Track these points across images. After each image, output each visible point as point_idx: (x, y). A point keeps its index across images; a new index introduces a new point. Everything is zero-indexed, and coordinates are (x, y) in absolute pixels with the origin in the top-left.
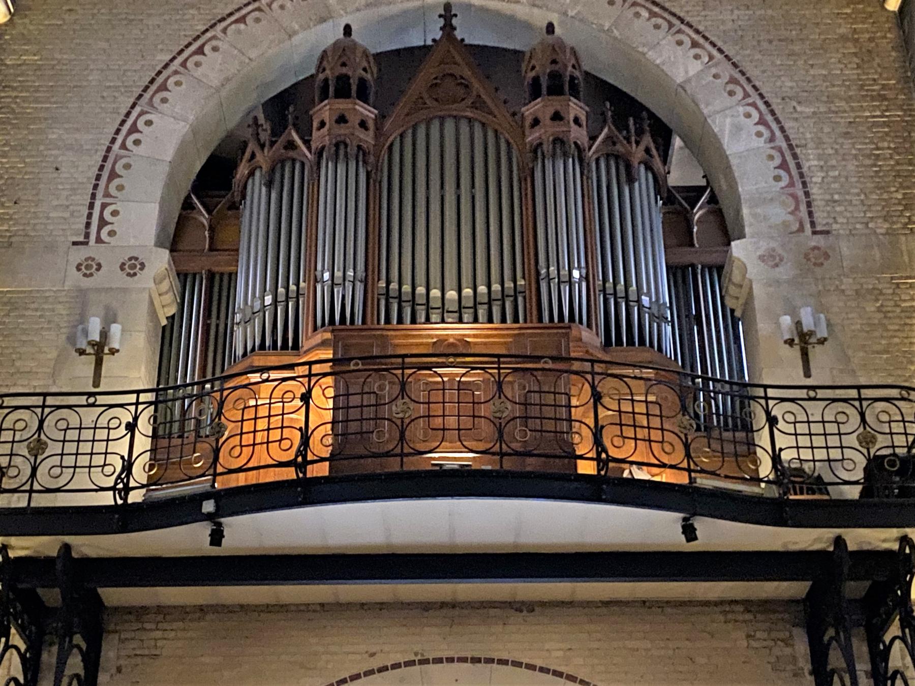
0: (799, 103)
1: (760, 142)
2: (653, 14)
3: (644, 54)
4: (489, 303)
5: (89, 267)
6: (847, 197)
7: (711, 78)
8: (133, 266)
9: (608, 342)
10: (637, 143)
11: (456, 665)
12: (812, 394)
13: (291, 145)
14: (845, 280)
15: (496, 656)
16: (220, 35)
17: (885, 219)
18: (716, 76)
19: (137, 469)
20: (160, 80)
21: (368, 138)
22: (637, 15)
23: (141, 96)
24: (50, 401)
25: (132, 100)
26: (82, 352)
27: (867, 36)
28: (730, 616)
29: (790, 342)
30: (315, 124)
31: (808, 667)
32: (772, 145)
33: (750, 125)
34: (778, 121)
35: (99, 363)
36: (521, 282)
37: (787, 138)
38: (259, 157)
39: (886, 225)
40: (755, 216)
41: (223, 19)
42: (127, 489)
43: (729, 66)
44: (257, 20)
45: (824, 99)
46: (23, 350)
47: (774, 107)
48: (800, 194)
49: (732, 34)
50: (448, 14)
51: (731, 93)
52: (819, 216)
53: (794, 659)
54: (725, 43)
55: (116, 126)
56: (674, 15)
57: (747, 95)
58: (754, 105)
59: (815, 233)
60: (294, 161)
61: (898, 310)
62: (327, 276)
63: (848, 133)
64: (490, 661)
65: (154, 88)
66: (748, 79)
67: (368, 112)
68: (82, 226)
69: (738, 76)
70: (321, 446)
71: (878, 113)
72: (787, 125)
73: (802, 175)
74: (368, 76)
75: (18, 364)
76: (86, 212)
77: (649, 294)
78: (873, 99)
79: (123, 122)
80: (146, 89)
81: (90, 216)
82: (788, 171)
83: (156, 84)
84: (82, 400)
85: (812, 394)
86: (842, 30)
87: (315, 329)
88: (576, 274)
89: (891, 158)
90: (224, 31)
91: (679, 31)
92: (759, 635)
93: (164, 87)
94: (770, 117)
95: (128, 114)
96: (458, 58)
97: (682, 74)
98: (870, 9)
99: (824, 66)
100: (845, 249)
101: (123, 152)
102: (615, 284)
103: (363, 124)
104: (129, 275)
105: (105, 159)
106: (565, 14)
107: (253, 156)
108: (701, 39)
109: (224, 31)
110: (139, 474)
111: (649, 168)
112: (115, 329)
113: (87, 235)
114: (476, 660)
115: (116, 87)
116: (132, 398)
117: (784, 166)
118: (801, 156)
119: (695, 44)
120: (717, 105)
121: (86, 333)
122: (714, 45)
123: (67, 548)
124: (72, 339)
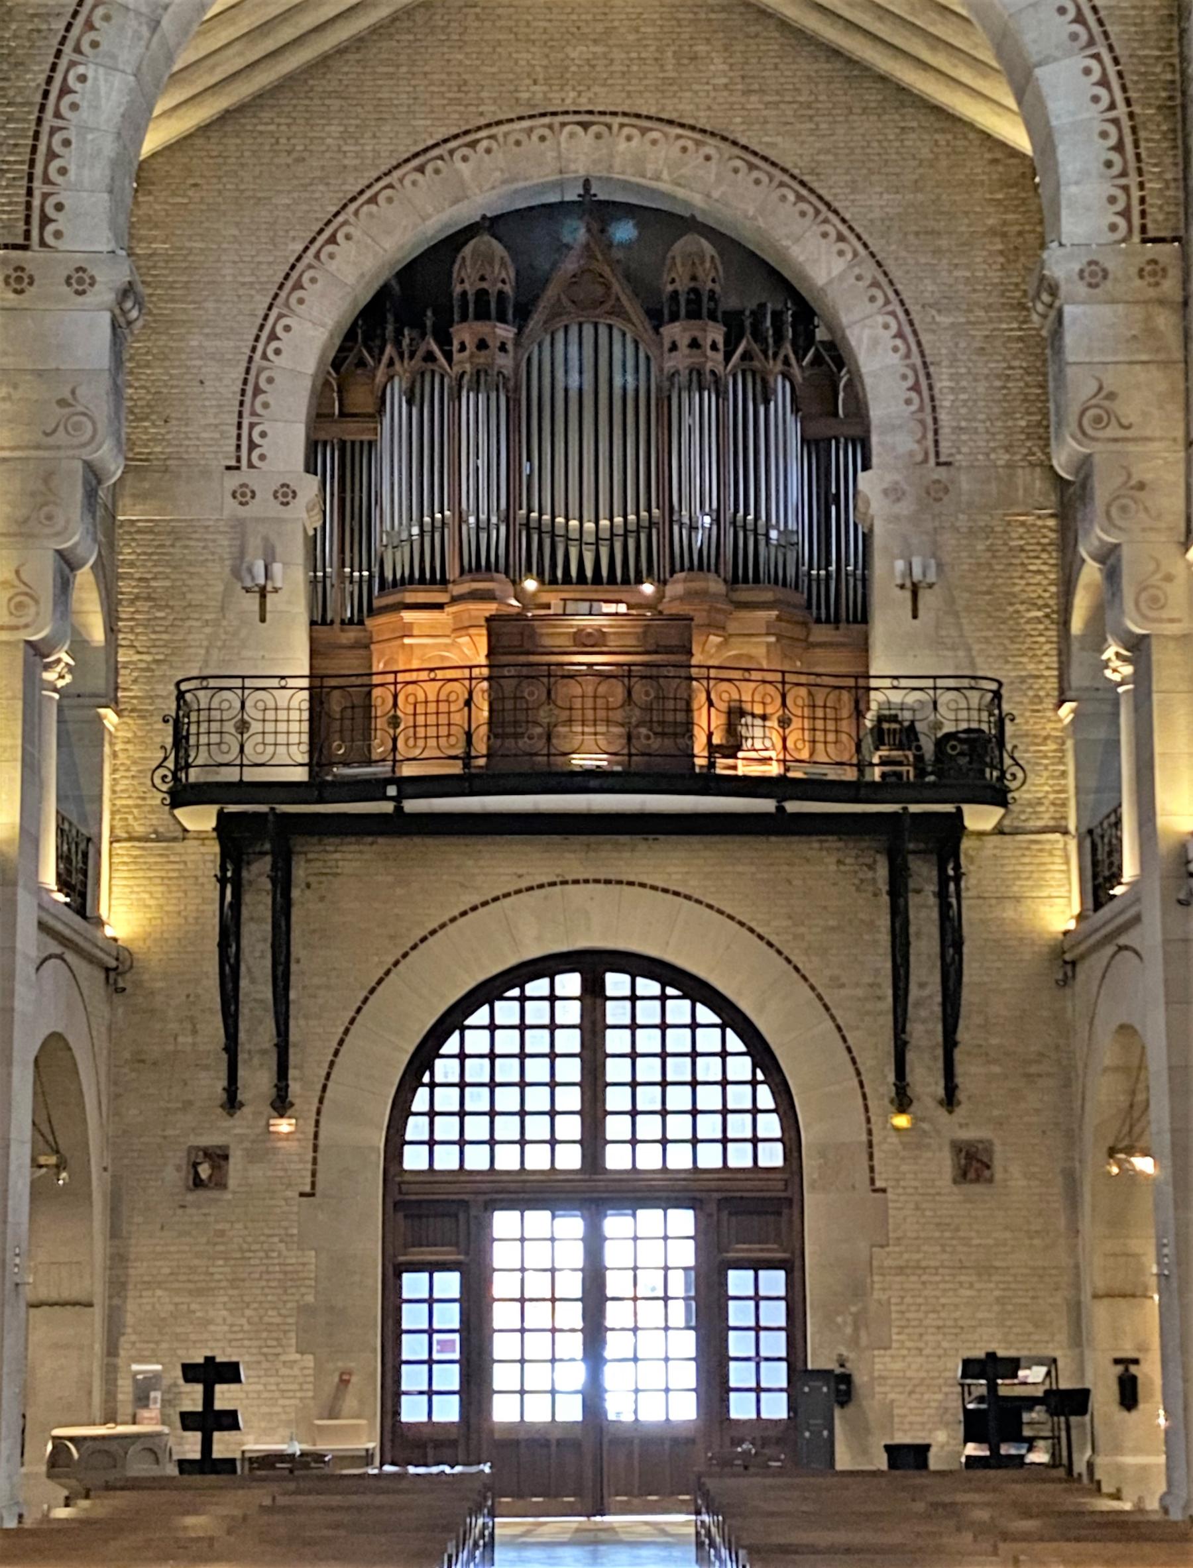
0: (939, 311)
1: (895, 359)
2: (800, 198)
3: (788, 248)
4: (625, 536)
5: (243, 495)
6: (975, 425)
7: (853, 280)
8: (285, 495)
9: (735, 580)
10: (775, 355)
11: (591, 886)
12: (895, 683)
13: (430, 357)
14: (961, 516)
15: (625, 878)
16: (352, 219)
17: (1008, 449)
18: (859, 278)
20: (295, 275)
21: (505, 362)
22: (783, 198)
23: (276, 296)
24: (248, 683)
25: (269, 300)
26: (248, 590)
27: (1017, 228)
28: (826, 845)
29: (902, 587)
30: (456, 345)
31: (885, 888)
32: (908, 362)
34: (915, 333)
36: (655, 511)
37: (923, 355)
38: (398, 366)
39: (1007, 457)
40: (881, 444)
41: (353, 199)
43: (871, 263)
44: (390, 200)
45: (964, 307)
46: (190, 582)
47: (913, 315)
48: (929, 421)
49: (878, 223)
50: (587, 183)
51: (872, 299)
52: (944, 445)
53: (874, 880)
54: (871, 234)
55: (255, 331)
56: (820, 198)
57: (887, 302)
58: (893, 314)
59: (938, 464)
60: (433, 372)
61: (1006, 549)
62: (472, 520)
63: (983, 349)
64: (620, 882)
65: (289, 284)
66: (891, 283)
67: (505, 332)
68: (233, 448)
71: (1015, 325)
72: (925, 338)
73: (932, 399)
74: (508, 288)
75: (189, 596)
76: (234, 432)
77: (777, 527)
78: (1013, 307)
79: (262, 327)
80: (281, 287)
81: (239, 437)
82: (919, 393)
83: (290, 280)
84: (275, 683)
85: (895, 683)
86: (990, 222)
87: (462, 572)
89: (1022, 379)
90: (356, 213)
91: (826, 221)
92: (848, 861)
93: (298, 286)
94: (909, 331)
95: (266, 317)
96: (600, 257)
97: (824, 273)
98: (1023, 195)
99: (968, 267)
100: (965, 483)
101: (265, 363)
102: (746, 513)
103: (503, 348)
104: (282, 504)
105: (248, 371)
106: (708, 196)
107: (391, 363)
108: (848, 232)
109: (356, 213)
111: (786, 376)
112: (277, 568)
113: (238, 460)
114: (608, 882)
115: (252, 283)
117: (915, 388)
118: (934, 376)
119: (841, 238)
120: (856, 315)
121: (250, 570)
122: (859, 238)
123: (273, 809)
124: (236, 573)
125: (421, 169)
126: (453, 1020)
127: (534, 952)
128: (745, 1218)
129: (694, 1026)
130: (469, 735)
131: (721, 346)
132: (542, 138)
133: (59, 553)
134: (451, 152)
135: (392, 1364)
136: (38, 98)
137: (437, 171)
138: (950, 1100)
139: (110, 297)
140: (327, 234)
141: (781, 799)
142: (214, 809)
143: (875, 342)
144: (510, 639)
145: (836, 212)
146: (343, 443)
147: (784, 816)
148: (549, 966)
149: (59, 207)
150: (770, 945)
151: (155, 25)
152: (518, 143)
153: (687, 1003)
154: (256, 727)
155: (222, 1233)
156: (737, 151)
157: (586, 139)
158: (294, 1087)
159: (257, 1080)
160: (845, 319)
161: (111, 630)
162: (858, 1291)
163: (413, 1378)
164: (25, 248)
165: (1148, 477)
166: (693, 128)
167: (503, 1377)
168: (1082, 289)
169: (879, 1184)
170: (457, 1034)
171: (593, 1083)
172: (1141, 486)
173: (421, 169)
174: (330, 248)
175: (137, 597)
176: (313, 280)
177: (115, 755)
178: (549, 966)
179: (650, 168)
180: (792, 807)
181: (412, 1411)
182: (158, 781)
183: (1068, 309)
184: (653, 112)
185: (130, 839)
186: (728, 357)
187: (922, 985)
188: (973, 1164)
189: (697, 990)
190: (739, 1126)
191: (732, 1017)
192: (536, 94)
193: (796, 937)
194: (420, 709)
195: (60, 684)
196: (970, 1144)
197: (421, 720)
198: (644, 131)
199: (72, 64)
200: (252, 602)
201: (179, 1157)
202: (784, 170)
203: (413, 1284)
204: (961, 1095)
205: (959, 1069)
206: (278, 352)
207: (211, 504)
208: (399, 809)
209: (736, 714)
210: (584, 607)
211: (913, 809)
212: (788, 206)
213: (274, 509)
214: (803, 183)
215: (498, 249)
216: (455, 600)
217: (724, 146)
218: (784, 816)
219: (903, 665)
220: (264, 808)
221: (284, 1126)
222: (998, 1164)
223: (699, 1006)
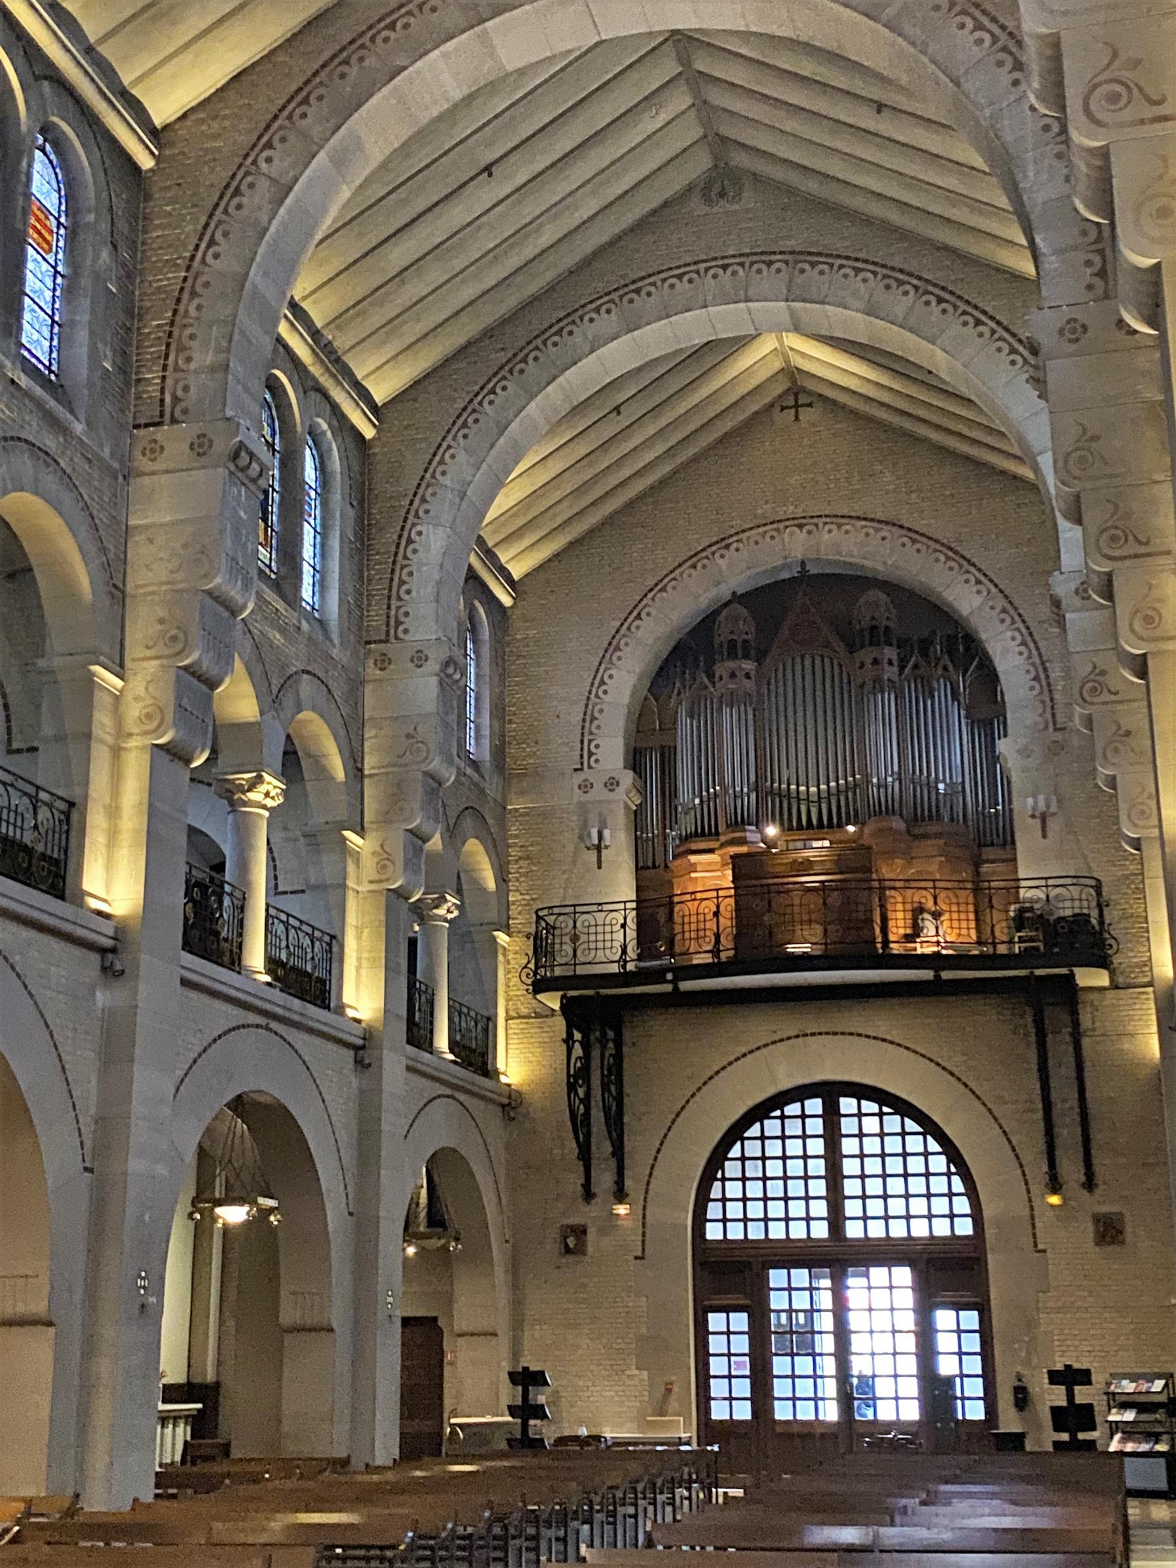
1: (1020, 661)
2: (948, 558)
5: (586, 787)
8: (612, 784)
9: (916, 819)
18: (992, 608)
19: (629, 950)
20: (615, 642)
22: (937, 560)
24: (578, 909)
33: (1014, 647)
34: (1035, 642)
35: (599, 852)
37: (1040, 655)
42: (626, 962)
50: (803, 563)
52: (1060, 718)
57: (1013, 622)
58: (1018, 629)
59: (1056, 730)
66: (1016, 609)
67: (749, 666)
69: (1008, 606)
70: (727, 942)
73: (1049, 685)
83: (612, 646)
84: (595, 908)
88: (890, 779)
91: (968, 572)
93: (617, 649)
95: (597, 671)
103: (748, 676)
107: (679, 694)
108: (984, 577)
110: (632, 953)
114: (836, 1034)
116: (622, 906)
117: (1036, 678)
119: (978, 582)
121: (589, 836)
122: (991, 581)
124: (581, 838)
125: (694, 566)
126: (736, 1133)
127: (786, 1084)
128: (947, 1272)
129: (903, 1134)
130: (717, 936)
131: (896, 663)
132: (772, 538)
133: (410, 831)
134: (713, 553)
135: (704, 1377)
136: (393, 548)
137: (704, 567)
138: (1090, 1184)
139: (437, 667)
140: (635, 613)
141: (937, 970)
142: (560, 993)
143: (1006, 651)
144: (747, 870)
145: (974, 565)
146: (662, 747)
147: (941, 985)
148: (800, 1093)
149: (407, 614)
150: (952, 1074)
151: (463, 496)
152: (756, 543)
153: (898, 1118)
154: (583, 938)
155: (585, 1286)
156: (904, 532)
157: (802, 535)
158: (628, 1183)
159: (604, 1179)
160: (983, 636)
161: (502, 878)
162: (1030, 1325)
163: (718, 1388)
164: (386, 641)
165: (1132, 727)
166: (872, 520)
167: (781, 1388)
168: (1077, 602)
169: (1040, 1247)
170: (739, 1144)
171: (834, 1177)
172: (1128, 733)
173: (694, 566)
174: (637, 622)
175: (521, 858)
176: (627, 644)
177: (508, 962)
178: (800, 1093)
179: (844, 550)
180: (946, 975)
181: (719, 1412)
182: (524, 978)
183: (1068, 616)
184: (845, 512)
185: (520, 1017)
186: (902, 668)
187: (1064, 1101)
188: (1109, 1231)
189: (904, 1108)
190: (940, 1206)
191: (930, 1128)
192: (765, 510)
193: (970, 1068)
194: (686, 920)
195: (450, 916)
196: (1106, 1215)
197: (687, 927)
198: (839, 526)
199: (414, 525)
200: (593, 855)
201: (554, 1233)
202: (937, 541)
203: (716, 1321)
204: (1099, 1179)
205: (1095, 1161)
206: (605, 692)
207: (566, 795)
208: (676, 988)
209: (919, 910)
210: (800, 844)
211: (1043, 974)
212: (940, 565)
213: (606, 795)
214: (951, 549)
215: (743, 611)
216: (722, 846)
217: (895, 529)
218: (941, 985)
219: (1038, 872)
220: (590, 992)
221: (622, 1210)
222: (1128, 1229)
223: (907, 1120)
